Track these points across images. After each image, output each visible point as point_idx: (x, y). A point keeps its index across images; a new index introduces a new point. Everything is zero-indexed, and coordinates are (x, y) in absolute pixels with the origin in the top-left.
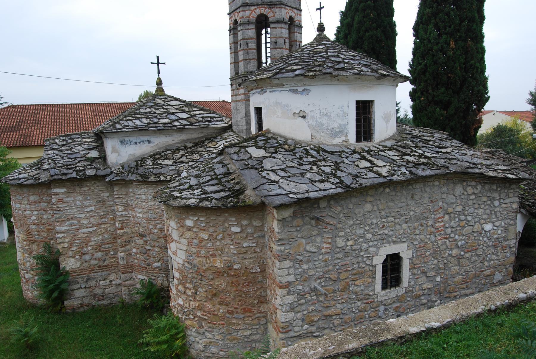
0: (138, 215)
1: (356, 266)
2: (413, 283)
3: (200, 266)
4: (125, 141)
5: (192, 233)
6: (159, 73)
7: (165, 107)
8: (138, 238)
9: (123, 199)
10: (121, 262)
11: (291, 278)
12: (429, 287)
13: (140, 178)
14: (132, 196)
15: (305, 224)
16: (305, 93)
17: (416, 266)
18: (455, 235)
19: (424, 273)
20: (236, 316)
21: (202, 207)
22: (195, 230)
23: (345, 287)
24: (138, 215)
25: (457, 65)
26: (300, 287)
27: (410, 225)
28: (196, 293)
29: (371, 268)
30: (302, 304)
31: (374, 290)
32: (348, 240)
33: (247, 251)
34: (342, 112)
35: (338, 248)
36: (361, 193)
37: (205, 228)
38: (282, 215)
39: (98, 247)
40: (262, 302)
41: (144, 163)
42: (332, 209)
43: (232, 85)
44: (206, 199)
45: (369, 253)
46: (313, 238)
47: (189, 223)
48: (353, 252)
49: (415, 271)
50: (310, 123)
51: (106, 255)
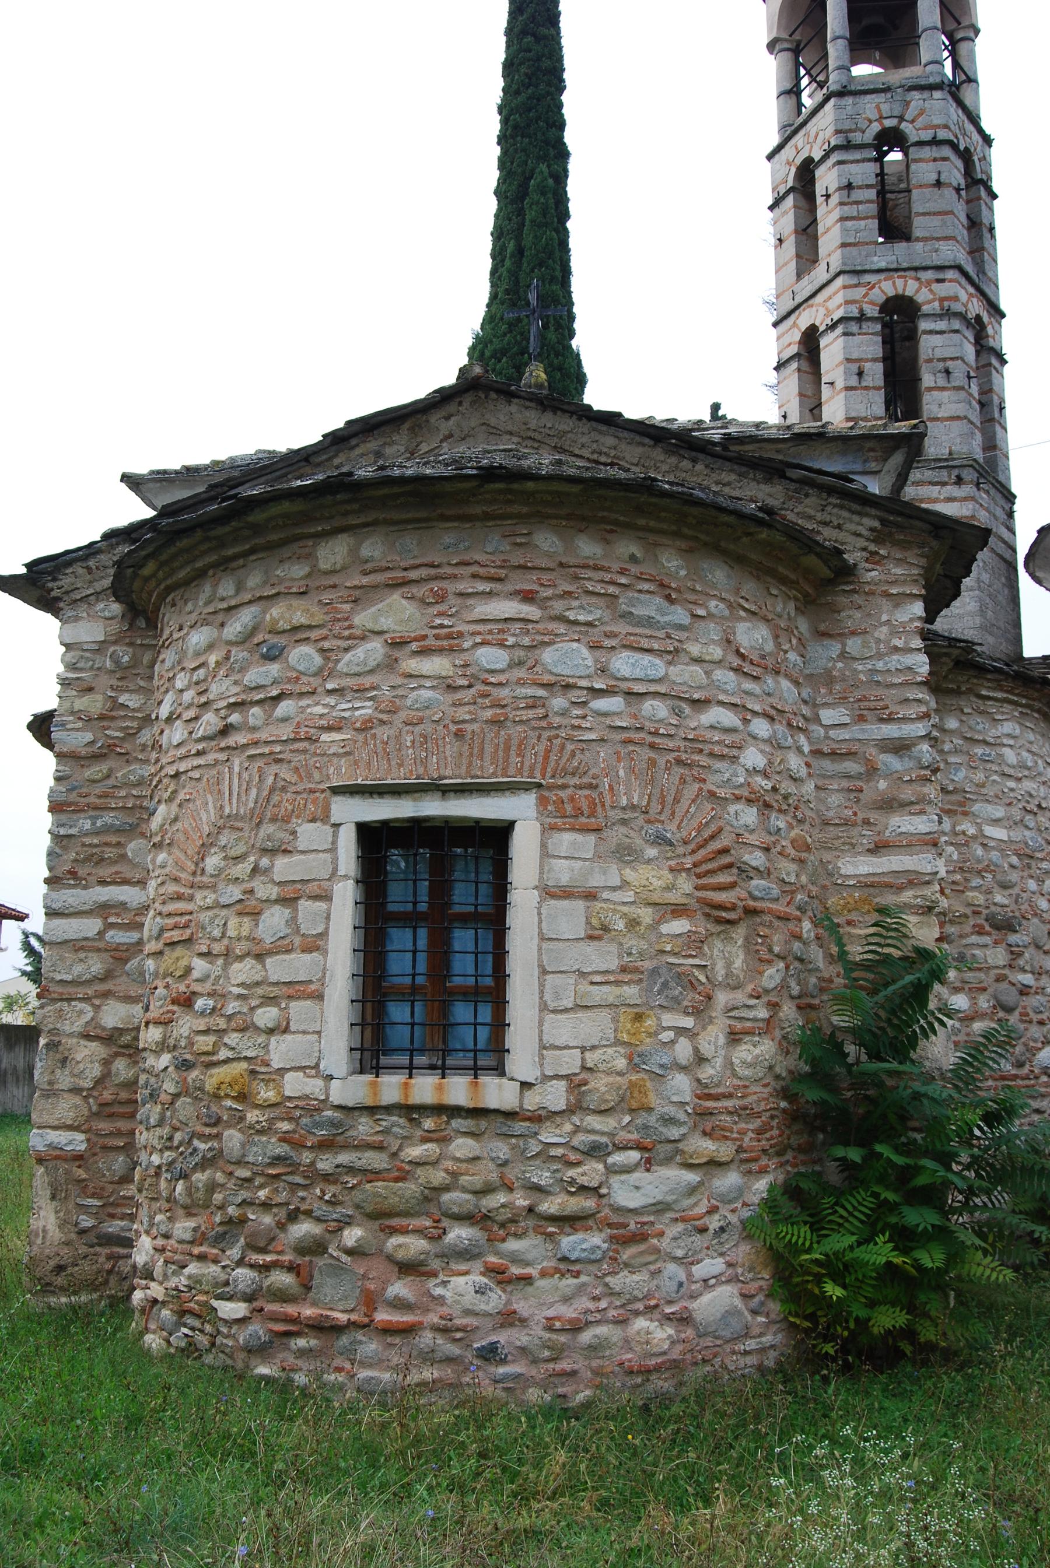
0: (990, 831)
8: (987, 940)
24: (990, 831)
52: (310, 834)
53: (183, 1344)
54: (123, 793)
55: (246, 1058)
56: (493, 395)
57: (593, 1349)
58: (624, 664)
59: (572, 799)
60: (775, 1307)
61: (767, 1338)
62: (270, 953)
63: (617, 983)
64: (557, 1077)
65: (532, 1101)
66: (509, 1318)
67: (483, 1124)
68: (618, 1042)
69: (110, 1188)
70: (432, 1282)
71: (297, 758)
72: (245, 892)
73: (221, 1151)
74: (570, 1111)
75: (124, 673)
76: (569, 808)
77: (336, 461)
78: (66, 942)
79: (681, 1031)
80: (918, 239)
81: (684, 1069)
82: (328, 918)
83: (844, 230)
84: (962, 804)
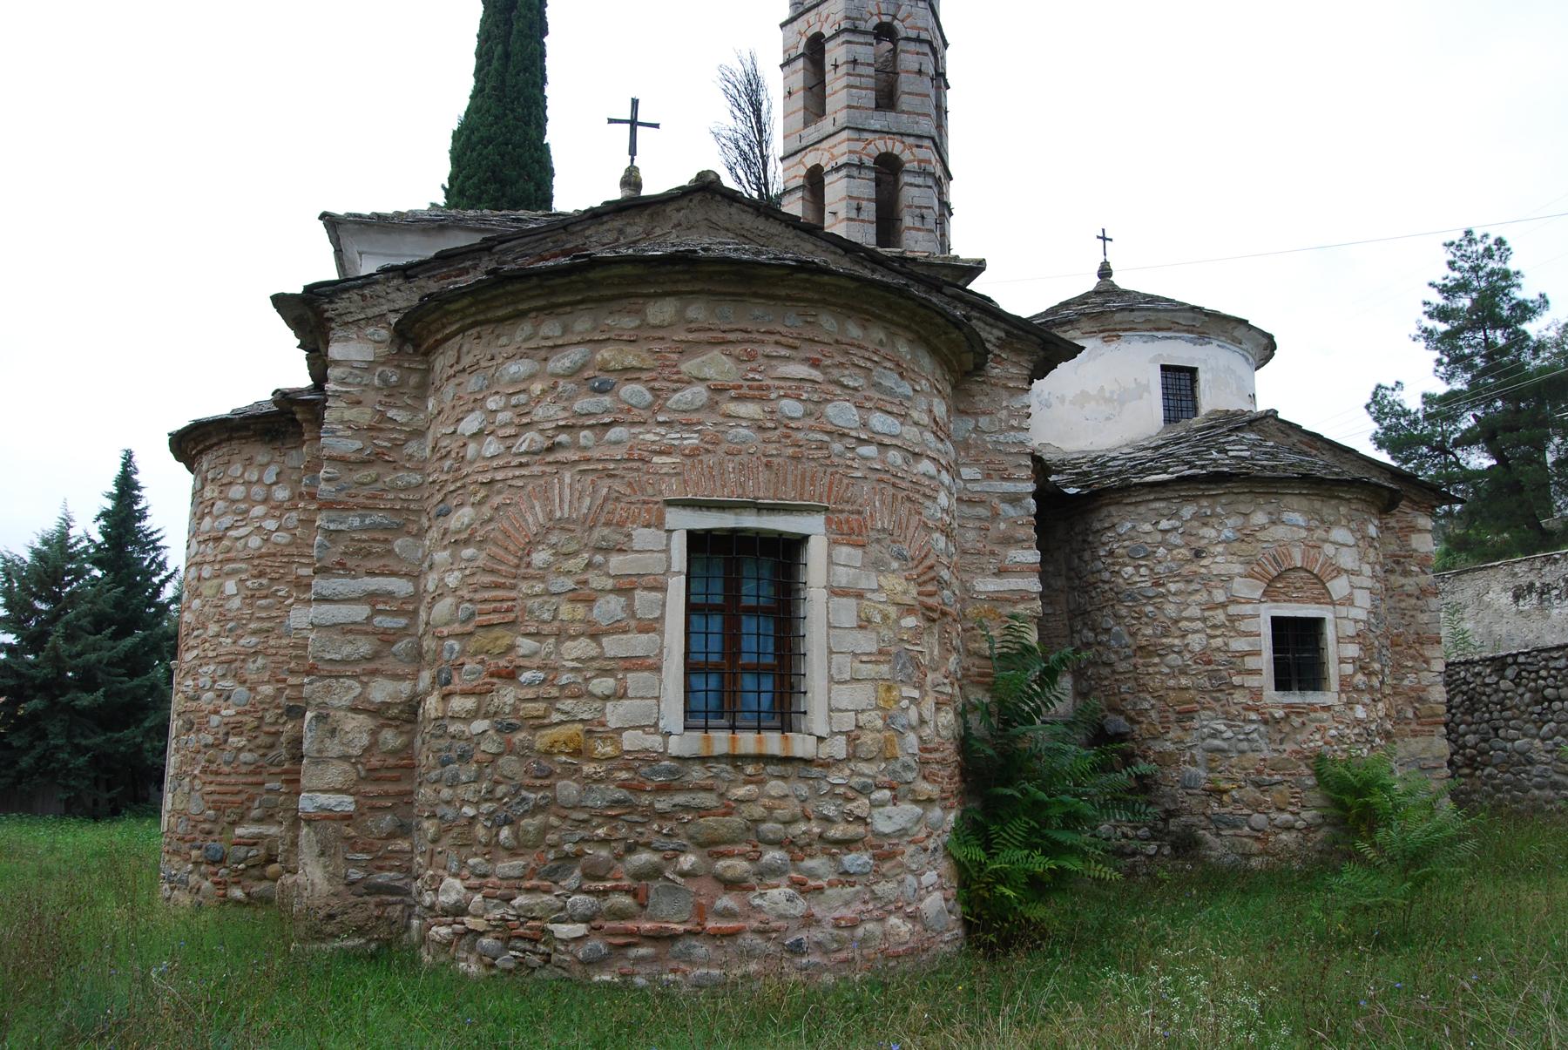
6: (633, 151)
52: (643, 537)
53: (511, 965)
54: (391, 496)
55: (582, 721)
56: (718, 198)
57: (864, 941)
58: (879, 422)
59: (847, 521)
60: (958, 908)
61: (951, 932)
62: (607, 633)
63: (877, 662)
64: (840, 733)
65: (825, 751)
66: (809, 920)
67: (790, 769)
68: (878, 708)
69: (379, 844)
70: (751, 895)
71: (630, 475)
72: (578, 583)
73: (555, 798)
74: (848, 759)
75: (391, 391)
76: (845, 527)
77: (588, 233)
78: (335, 625)
79: (912, 700)
80: (903, 112)
81: (913, 728)
82: (664, 605)
83: (850, 95)
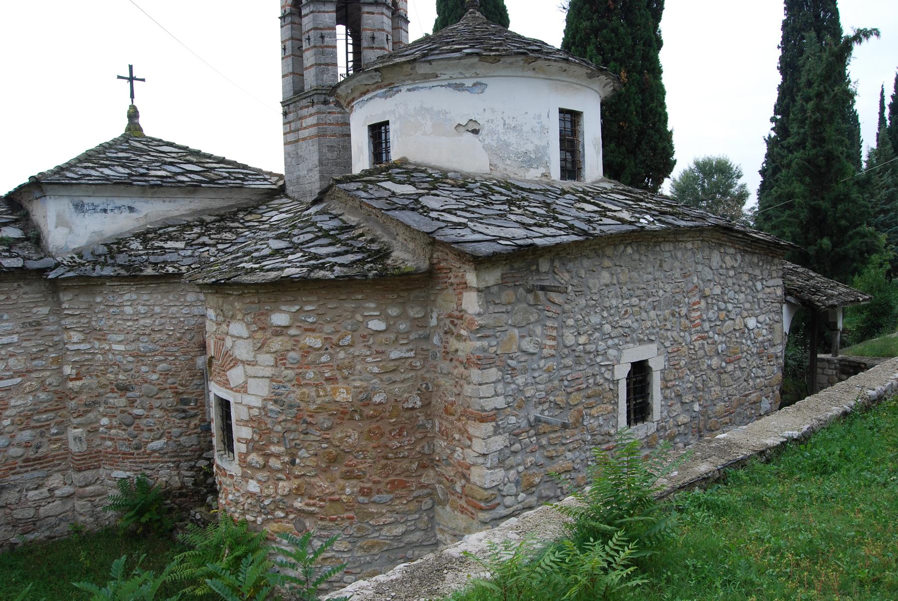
0: (115, 347)
1: (591, 381)
2: (665, 413)
3: (303, 405)
4: (83, 205)
5: (286, 339)
6: (132, 96)
7: (152, 153)
8: (115, 395)
9: (81, 317)
10: (74, 447)
11: (500, 402)
12: (686, 420)
13: (123, 272)
14: (102, 311)
15: (518, 300)
16: (476, 89)
17: (670, 384)
18: (715, 333)
19: (679, 396)
20: (376, 497)
21: (318, 280)
22: (293, 331)
23: (577, 421)
24: (115, 347)
25: (633, 107)
26: (513, 420)
27: (659, 313)
28: (293, 463)
29: (612, 386)
30: (515, 453)
31: (615, 426)
32: (579, 334)
33: (398, 367)
34: (539, 126)
35: (566, 347)
36: (596, 252)
37: (314, 326)
38: (484, 280)
39: (25, 420)
40: (424, 467)
41: (124, 247)
42: (557, 277)
43: (285, 114)
44: (322, 267)
45: (608, 360)
46: (531, 326)
47: (280, 319)
48: (587, 356)
49: (668, 391)
50: (486, 142)
51: (42, 435)
84: (104, 335)
